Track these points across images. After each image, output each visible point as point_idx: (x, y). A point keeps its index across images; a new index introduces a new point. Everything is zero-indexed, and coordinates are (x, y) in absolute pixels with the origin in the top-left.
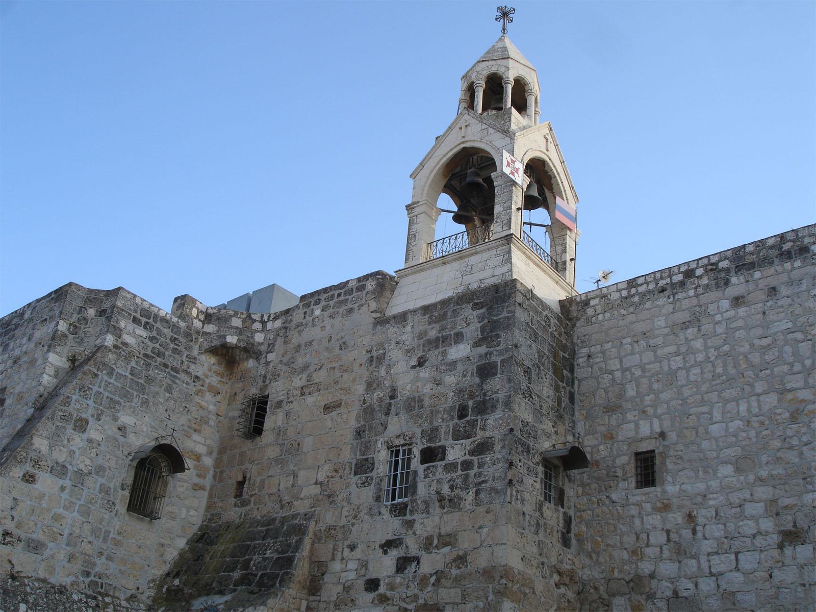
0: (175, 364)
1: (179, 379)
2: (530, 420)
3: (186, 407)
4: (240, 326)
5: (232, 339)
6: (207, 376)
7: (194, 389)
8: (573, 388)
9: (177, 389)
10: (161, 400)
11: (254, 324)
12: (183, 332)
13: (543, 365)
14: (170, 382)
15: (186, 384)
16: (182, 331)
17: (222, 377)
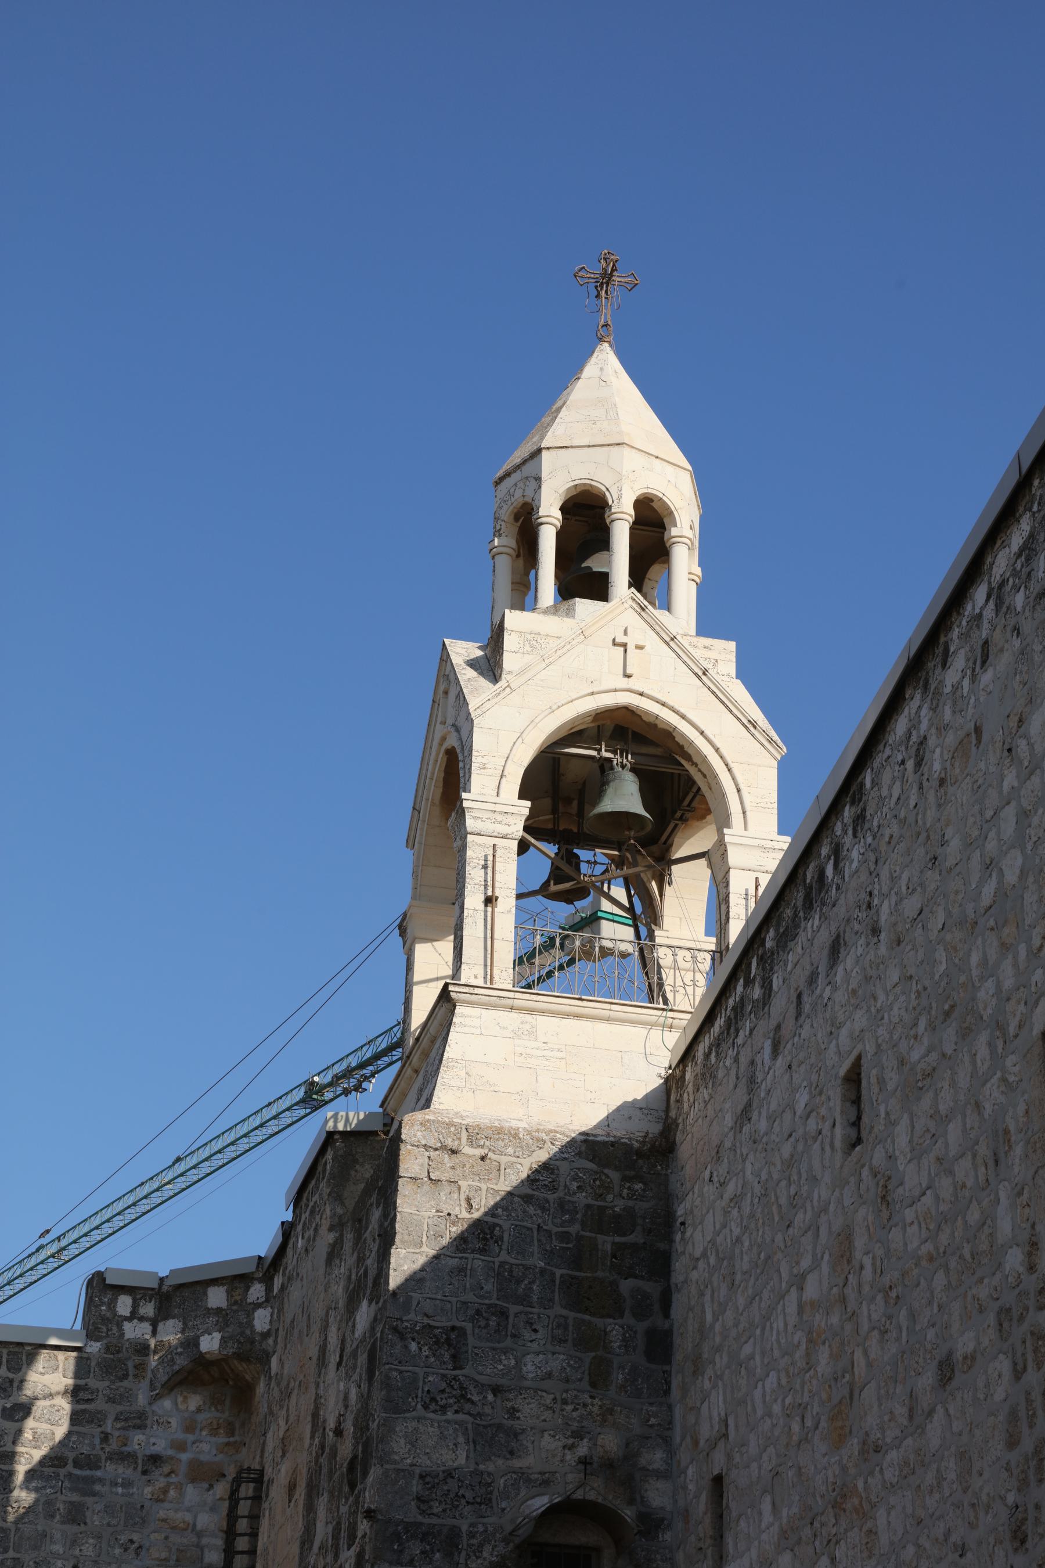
0: (86, 1450)
1: (100, 1480)
2: (462, 1460)
3: (132, 1541)
4: (224, 1305)
5: (210, 1344)
6: (181, 1447)
7: (148, 1490)
8: (667, 1315)
9: (99, 1507)
10: (58, 1548)
11: (252, 1290)
12: (98, 1364)
13: (524, 1300)
14: (75, 1497)
15: (123, 1485)
16: (93, 1364)
17: (231, 1432)
